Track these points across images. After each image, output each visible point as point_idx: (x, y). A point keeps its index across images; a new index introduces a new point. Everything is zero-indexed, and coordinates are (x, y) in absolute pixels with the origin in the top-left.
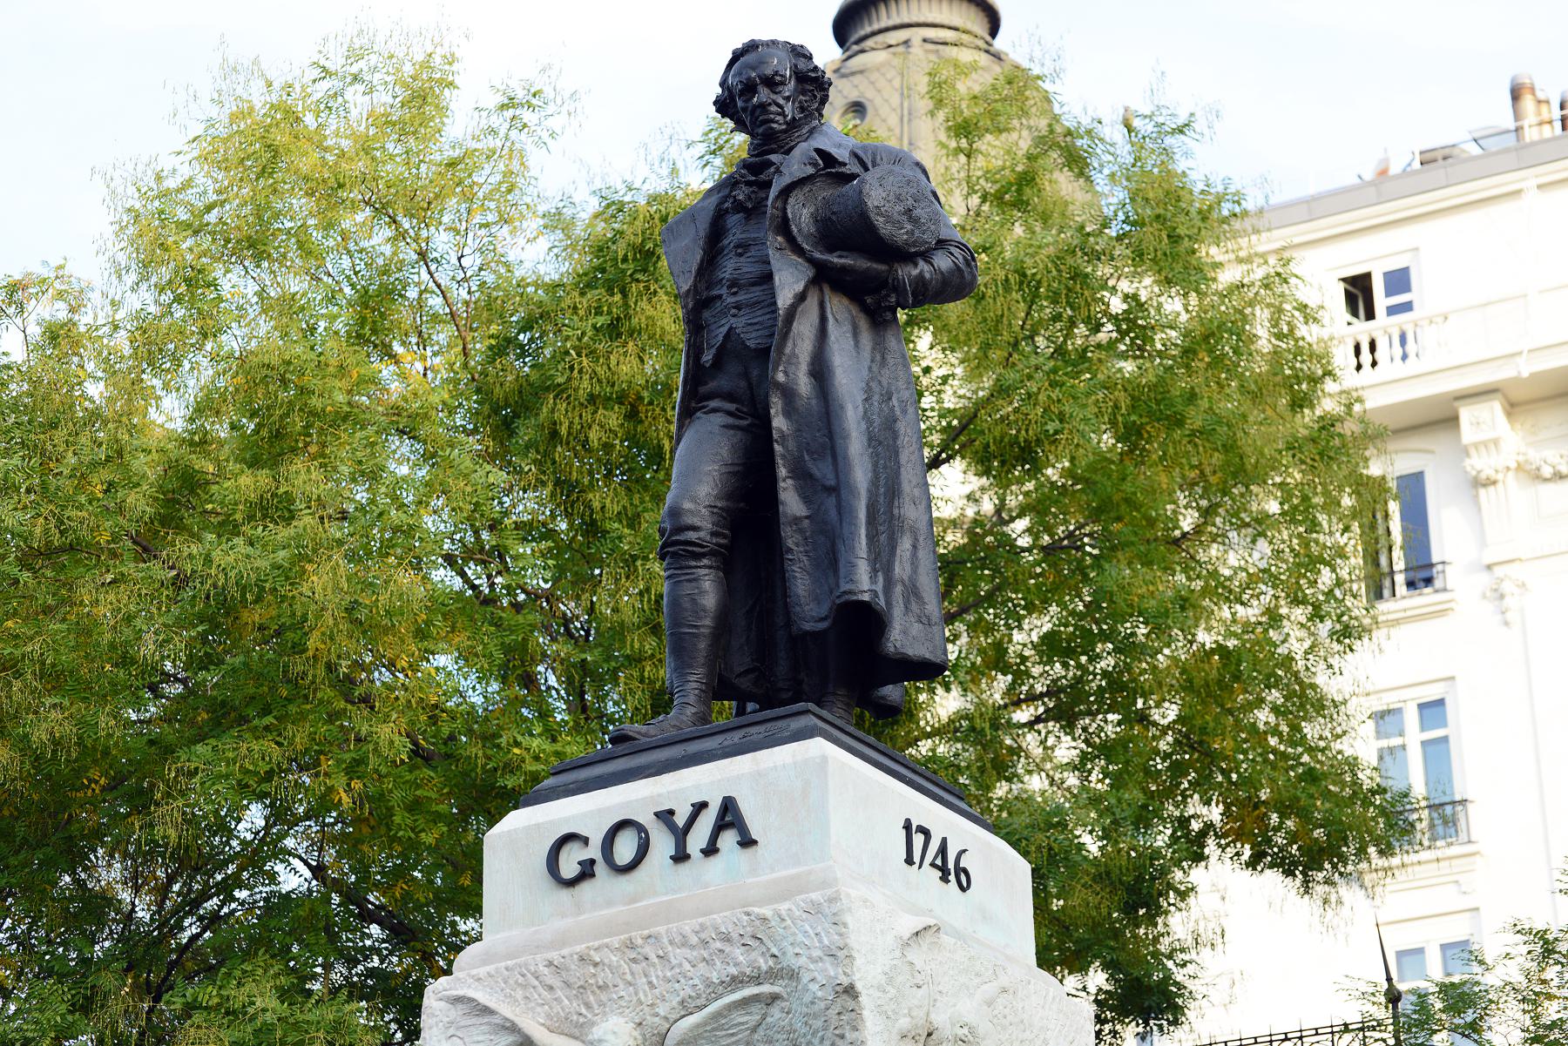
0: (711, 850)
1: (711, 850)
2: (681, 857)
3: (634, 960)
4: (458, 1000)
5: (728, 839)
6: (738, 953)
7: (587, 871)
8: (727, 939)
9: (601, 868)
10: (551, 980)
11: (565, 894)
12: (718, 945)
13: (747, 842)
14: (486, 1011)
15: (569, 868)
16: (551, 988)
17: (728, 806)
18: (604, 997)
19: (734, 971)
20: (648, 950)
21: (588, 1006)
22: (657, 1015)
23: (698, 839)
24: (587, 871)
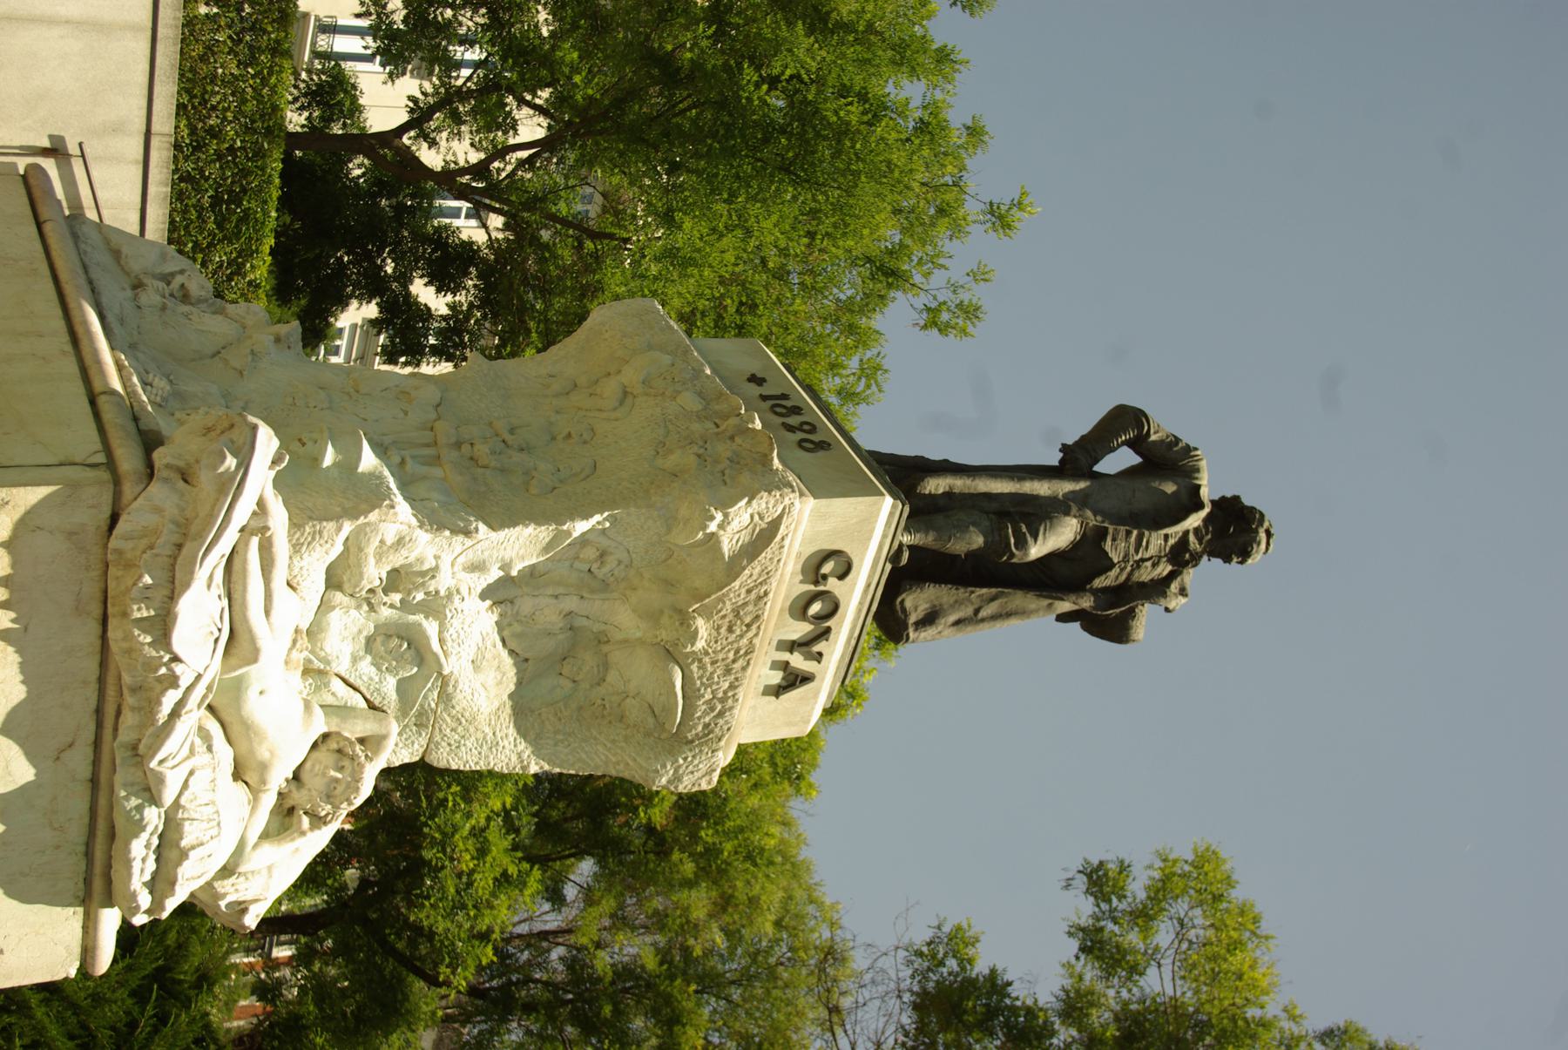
2: (792, 646)
3: (737, 652)
8: (721, 714)
13: (778, 691)
16: (749, 591)
17: (806, 679)
18: (723, 630)
23: (797, 661)
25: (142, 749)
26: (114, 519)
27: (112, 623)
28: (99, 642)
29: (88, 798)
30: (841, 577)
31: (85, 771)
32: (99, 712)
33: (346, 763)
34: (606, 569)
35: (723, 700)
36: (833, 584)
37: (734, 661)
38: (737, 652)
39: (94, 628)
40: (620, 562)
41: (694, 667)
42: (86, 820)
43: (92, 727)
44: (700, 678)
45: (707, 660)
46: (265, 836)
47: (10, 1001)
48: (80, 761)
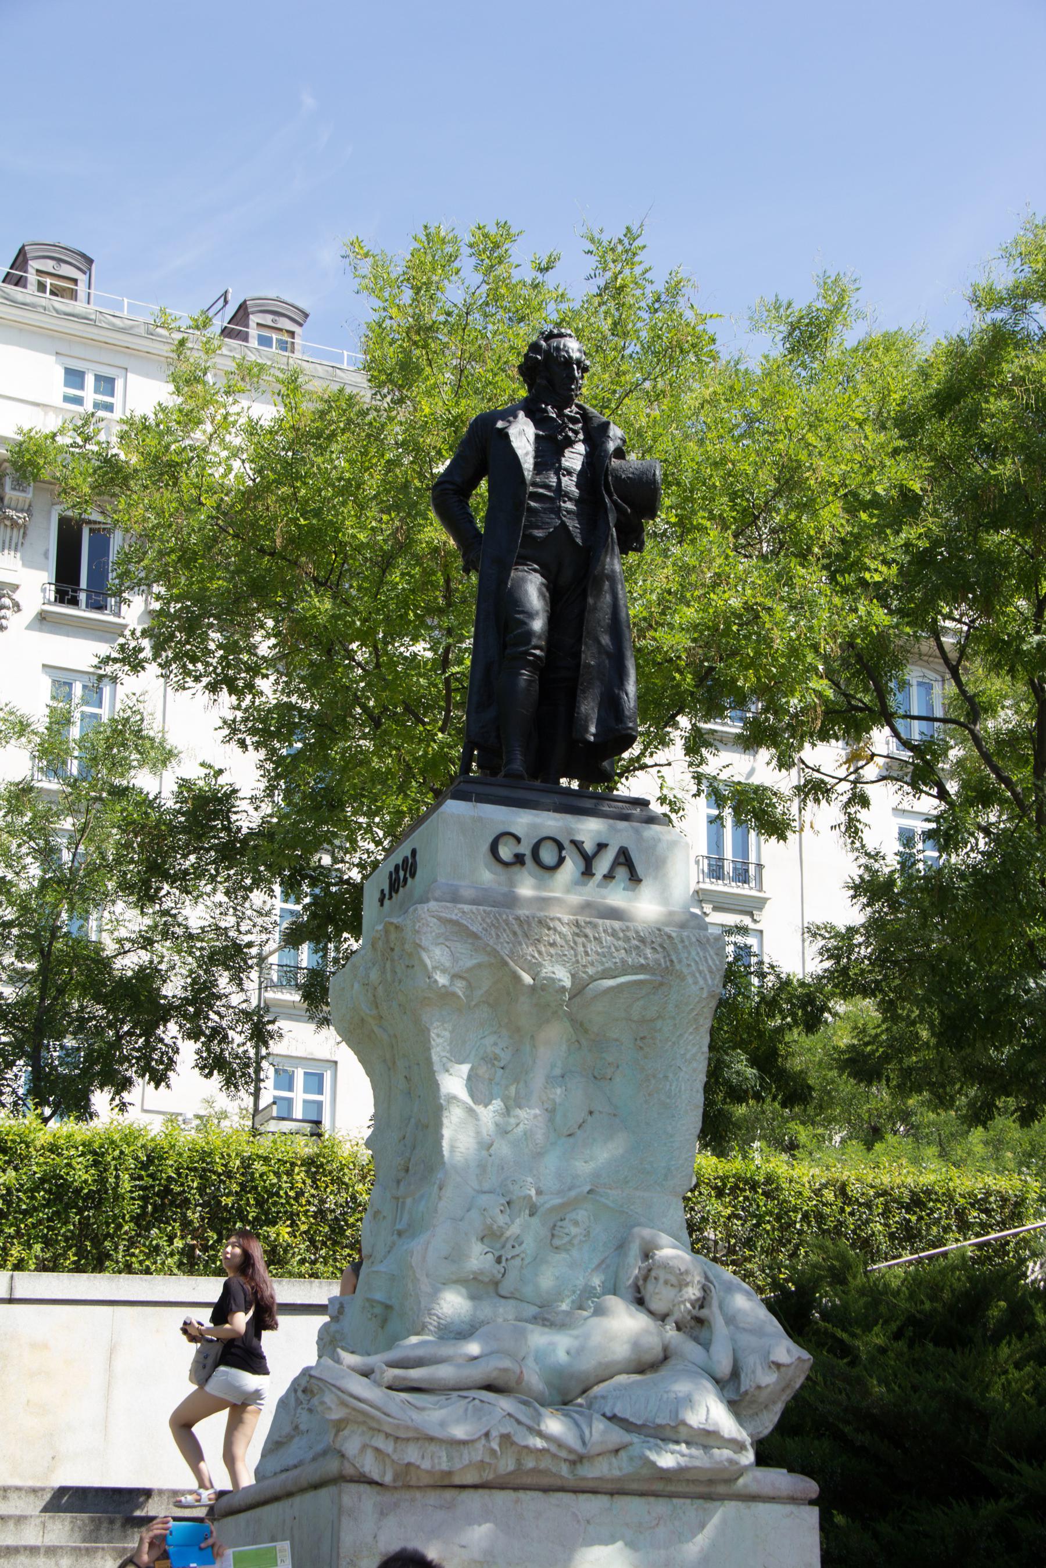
0: (609, 877)
1: (609, 877)
2: (588, 872)
4: (451, 921)
5: (622, 872)
6: (648, 952)
7: (519, 859)
8: (643, 940)
9: (528, 859)
10: (516, 928)
11: (499, 868)
12: (636, 942)
14: (475, 936)
15: (505, 852)
16: (515, 934)
18: (552, 951)
19: (643, 961)
20: (588, 931)
21: (540, 953)
22: (585, 972)
23: (602, 865)
24: (519, 859)
25: (572, 1457)
26: (372, 1482)
27: (457, 1481)
28: (481, 1491)
29: (628, 1498)
30: (518, 840)
31: (603, 1501)
32: (546, 1490)
33: (653, 1274)
34: (502, 1055)
35: (627, 939)
36: (525, 849)
37: (586, 936)
38: (577, 935)
39: (466, 1495)
40: (496, 1044)
41: (591, 971)
42: (652, 1499)
43: (560, 1495)
44: (602, 963)
45: (584, 962)
46: (706, 1346)
47: (826, 1559)
48: (590, 1505)
